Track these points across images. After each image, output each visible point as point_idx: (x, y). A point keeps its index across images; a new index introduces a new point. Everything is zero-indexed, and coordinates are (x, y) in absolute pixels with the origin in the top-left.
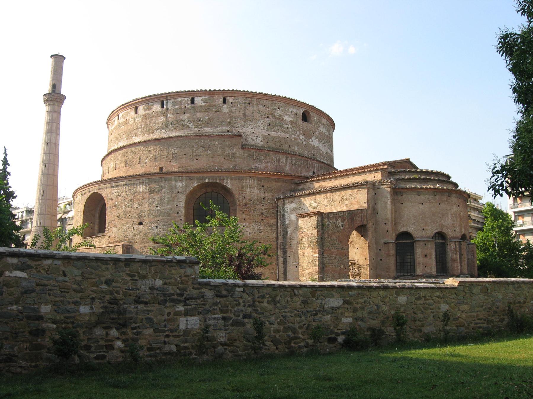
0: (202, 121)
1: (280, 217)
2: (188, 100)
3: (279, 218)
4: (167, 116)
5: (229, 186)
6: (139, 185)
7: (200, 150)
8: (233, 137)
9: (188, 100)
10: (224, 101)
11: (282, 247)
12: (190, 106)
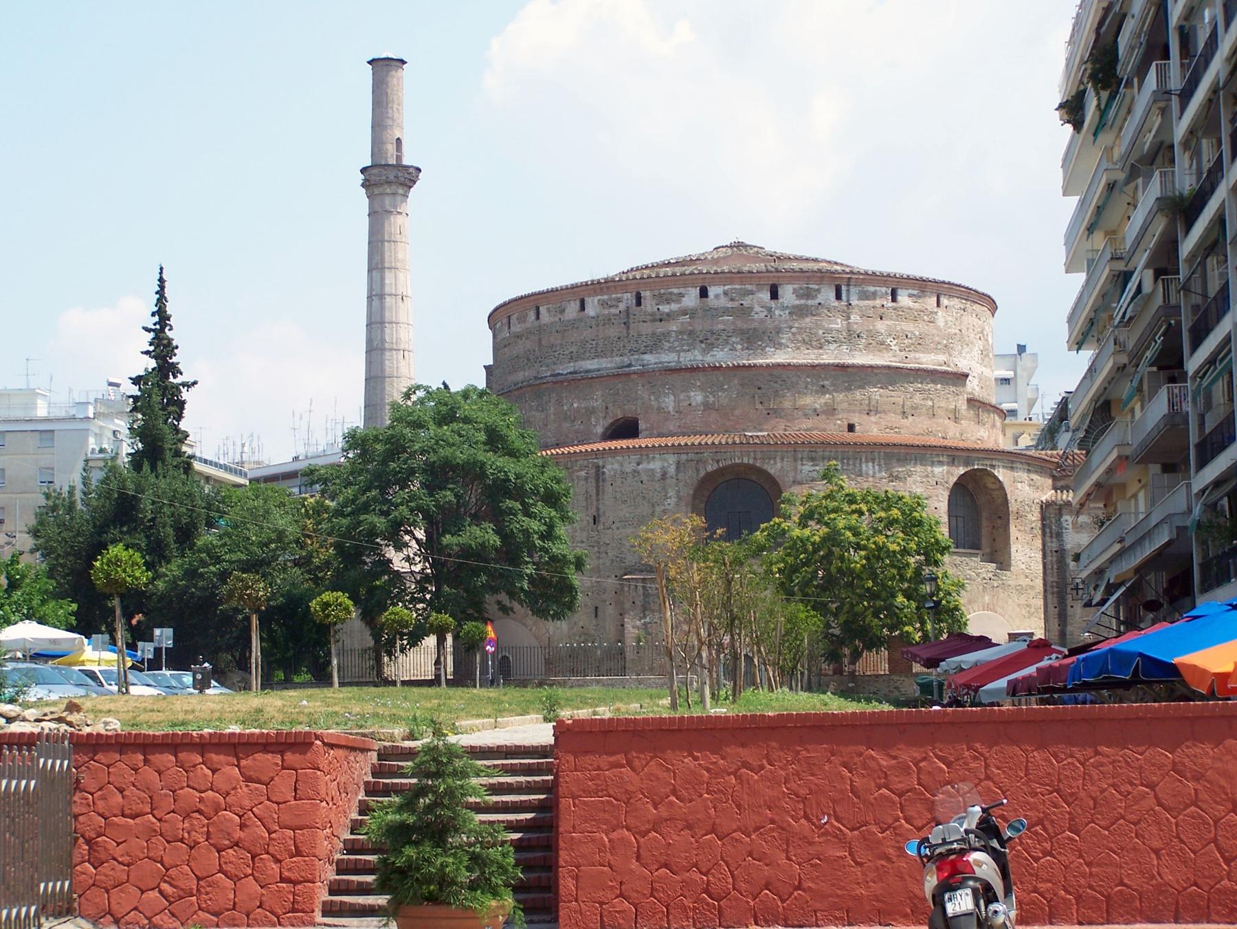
0: (911, 338)
1: (1051, 537)
2: (887, 293)
3: (1048, 539)
4: (849, 318)
5: (1001, 478)
6: (867, 462)
7: (918, 398)
8: (958, 378)
9: (887, 293)
10: (938, 305)
11: (1056, 590)
12: (891, 304)
